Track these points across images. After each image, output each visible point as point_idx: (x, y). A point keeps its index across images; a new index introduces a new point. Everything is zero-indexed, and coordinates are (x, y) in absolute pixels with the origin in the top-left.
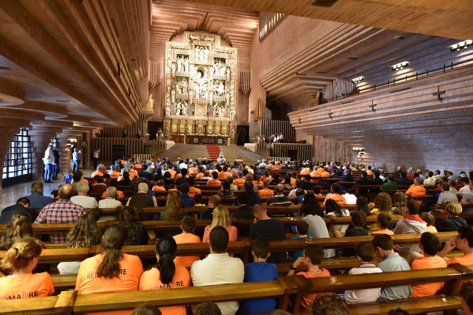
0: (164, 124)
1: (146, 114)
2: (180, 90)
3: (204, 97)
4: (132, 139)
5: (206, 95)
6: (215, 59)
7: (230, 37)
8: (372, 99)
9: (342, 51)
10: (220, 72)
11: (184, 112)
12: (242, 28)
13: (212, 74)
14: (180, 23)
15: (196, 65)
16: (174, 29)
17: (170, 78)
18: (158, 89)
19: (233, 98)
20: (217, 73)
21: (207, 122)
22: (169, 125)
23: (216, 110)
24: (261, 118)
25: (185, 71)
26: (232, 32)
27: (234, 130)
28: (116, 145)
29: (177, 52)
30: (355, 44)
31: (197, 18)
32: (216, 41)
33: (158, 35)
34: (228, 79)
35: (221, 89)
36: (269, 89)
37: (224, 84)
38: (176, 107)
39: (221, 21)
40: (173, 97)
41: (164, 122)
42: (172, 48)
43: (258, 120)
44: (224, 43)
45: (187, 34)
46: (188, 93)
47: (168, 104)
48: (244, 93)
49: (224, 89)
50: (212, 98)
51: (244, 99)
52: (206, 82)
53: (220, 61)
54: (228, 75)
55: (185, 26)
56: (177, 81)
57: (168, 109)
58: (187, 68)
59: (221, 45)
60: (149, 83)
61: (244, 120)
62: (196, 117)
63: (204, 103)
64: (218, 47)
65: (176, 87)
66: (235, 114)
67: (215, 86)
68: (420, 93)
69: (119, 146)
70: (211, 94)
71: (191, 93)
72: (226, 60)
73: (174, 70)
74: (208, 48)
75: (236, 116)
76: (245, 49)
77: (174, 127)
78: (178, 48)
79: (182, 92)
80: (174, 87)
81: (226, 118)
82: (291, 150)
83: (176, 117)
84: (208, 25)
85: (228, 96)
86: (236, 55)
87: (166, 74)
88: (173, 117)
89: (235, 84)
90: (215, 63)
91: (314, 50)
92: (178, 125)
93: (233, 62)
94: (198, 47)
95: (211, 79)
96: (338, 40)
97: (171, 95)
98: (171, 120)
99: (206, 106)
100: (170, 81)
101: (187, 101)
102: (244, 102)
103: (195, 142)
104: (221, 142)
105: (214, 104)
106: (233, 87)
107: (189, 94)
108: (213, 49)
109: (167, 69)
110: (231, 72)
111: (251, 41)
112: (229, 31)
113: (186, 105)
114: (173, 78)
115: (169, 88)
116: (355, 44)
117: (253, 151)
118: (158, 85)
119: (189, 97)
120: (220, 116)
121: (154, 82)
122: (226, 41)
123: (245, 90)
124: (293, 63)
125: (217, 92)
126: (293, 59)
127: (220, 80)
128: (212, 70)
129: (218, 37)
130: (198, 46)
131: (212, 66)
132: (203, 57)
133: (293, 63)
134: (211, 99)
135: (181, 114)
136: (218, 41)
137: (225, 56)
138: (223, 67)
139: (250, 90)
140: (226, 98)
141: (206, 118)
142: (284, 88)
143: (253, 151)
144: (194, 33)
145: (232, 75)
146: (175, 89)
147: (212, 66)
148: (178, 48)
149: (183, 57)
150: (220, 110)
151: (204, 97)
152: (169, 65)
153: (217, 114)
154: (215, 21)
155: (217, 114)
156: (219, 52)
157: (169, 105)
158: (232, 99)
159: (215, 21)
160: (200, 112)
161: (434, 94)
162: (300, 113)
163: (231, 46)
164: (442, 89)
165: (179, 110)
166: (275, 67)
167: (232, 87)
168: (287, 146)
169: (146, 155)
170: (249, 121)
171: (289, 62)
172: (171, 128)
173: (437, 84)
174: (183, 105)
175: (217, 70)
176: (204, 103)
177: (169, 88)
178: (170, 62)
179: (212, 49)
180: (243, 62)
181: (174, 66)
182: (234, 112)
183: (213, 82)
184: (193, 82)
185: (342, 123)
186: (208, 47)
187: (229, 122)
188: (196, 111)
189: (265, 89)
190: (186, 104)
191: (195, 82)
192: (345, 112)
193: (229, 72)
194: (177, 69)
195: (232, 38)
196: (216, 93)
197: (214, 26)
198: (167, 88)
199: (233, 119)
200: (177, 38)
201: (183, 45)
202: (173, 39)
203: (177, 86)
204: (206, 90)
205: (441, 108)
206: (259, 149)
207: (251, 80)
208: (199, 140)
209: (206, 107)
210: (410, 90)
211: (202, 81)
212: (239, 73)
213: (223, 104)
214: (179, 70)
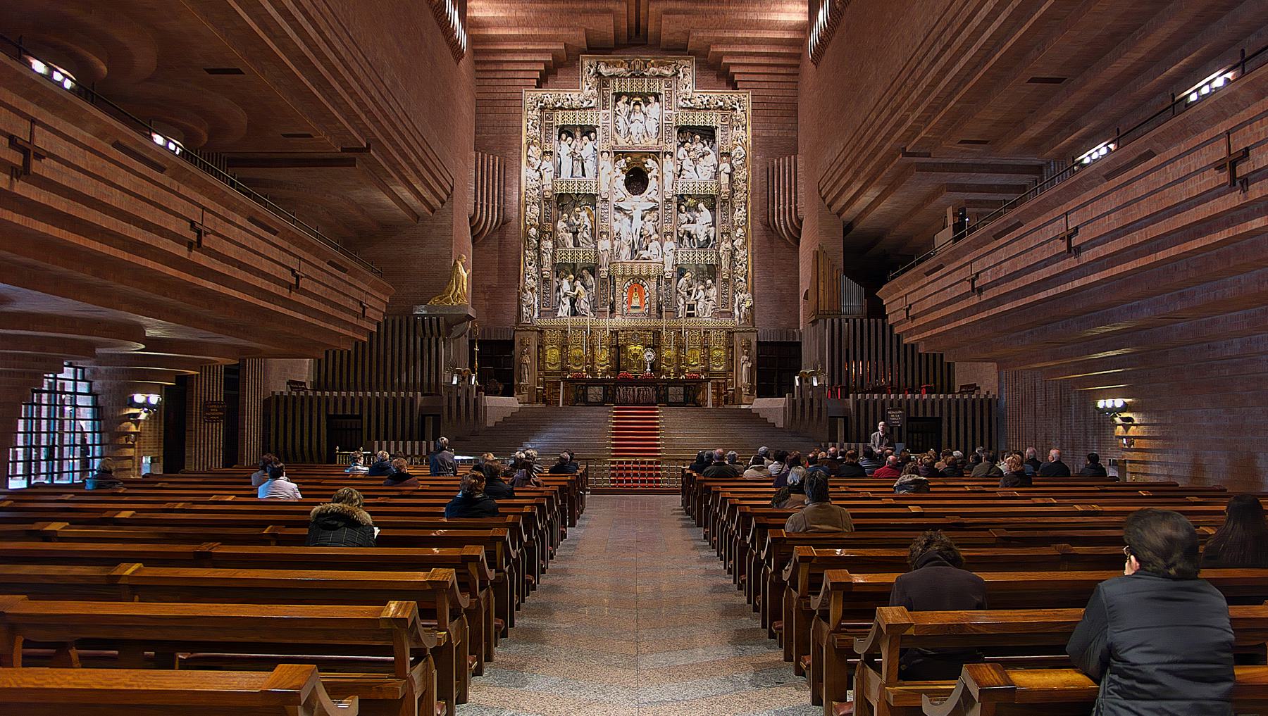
0: (517, 347)
3: (645, 254)
4: (411, 394)
5: (654, 246)
6: (681, 130)
7: (725, 61)
8: (1064, 208)
9: (997, 56)
10: (698, 170)
11: (583, 305)
12: (760, 26)
13: (669, 178)
14: (561, 31)
15: (618, 155)
16: (547, 51)
19: (743, 252)
20: (689, 175)
21: (657, 333)
22: (533, 348)
23: (689, 293)
25: (584, 175)
26: (729, 42)
27: (745, 357)
28: (336, 416)
29: (560, 119)
30: (1027, 26)
31: (609, 11)
32: (681, 75)
33: (499, 75)
34: (725, 189)
35: (702, 224)
36: (848, 215)
37: (712, 209)
38: (558, 290)
39: (685, 12)
40: (547, 258)
41: (517, 341)
42: (542, 109)
44: (711, 78)
45: (586, 63)
47: (531, 283)
48: (776, 239)
49: (714, 225)
50: (672, 256)
52: (653, 205)
54: (724, 179)
55: (577, 37)
56: (561, 208)
57: (532, 299)
58: (589, 166)
59: (699, 85)
62: (618, 321)
64: (687, 91)
65: (555, 229)
66: (748, 304)
67: (684, 217)
68: (1180, 168)
69: (344, 416)
70: (670, 244)
71: (604, 244)
72: (718, 134)
73: (548, 177)
74: (657, 100)
76: (779, 93)
77: (553, 354)
78: (560, 108)
79: (576, 244)
81: (717, 313)
82: (916, 419)
83: (554, 322)
84: (652, 28)
86: (749, 112)
87: (523, 190)
88: (546, 322)
90: (683, 144)
91: (925, 64)
92: (564, 346)
93: (740, 138)
94: (625, 99)
95: (668, 196)
96: (977, 21)
97: (539, 254)
98: (541, 332)
100: (536, 209)
103: (591, 398)
104: (681, 399)
105: (681, 272)
107: (596, 247)
108: (674, 100)
109: (527, 173)
110: (733, 169)
111: (797, 66)
112: (720, 41)
113: (589, 284)
114: (548, 201)
115: (533, 231)
116: (1027, 26)
117: (780, 424)
119: (597, 257)
121: (490, 217)
122: (717, 72)
123: (782, 222)
124: (884, 116)
125: (690, 236)
126: (882, 104)
127: (699, 198)
128: (669, 165)
129: (687, 63)
130: (625, 94)
131: (672, 155)
132: (644, 126)
133: (884, 116)
134: (669, 260)
135: (574, 313)
136: (688, 77)
137: (713, 119)
139: (800, 222)
141: (653, 323)
142: (885, 206)
143: (780, 424)
144: (610, 58)
146: (553, 234)
147: (672, 155)
148: (560, 108)
149: (578, 134)
150: (701, 293)
151: (645, 254)
152: (532, 160)
153: (691, 308)
154: (668, 12)
155: (691, 308)
156: (690, 108)
157: (534, 284)
158: (741, 254)
159: (668, 12)
160: (636, 302)
161: (1219, 167)
162: (907, 285)
163: (733, 85)
164: (1238, 145)
165: (567, 302)
166: (846, 140)
167: (739, 215)
168: (904, 403)
169: (409, 443)
171: (874, 115)
172: (541, 359)
173: (1221, 128)
174: (578, 283)
175: (687, 163)
177: (533, 231)
179: (669, 101)
180: (774, 133)
185: (1007, 307)
186: (657, 97)
187: (730, 333)
188: (619, 301)
189: (839, 214)
191: (619, 209)
192: (1006, 269)
193: (728, 170)
194: (558, 173)
195: (732, 61)
197: (670, 28)
200: (561, 77)
201: (574, 96)
202: (546, 81)
203: (561, 225)
205: (1249, 217)
206: (798, 417)
208: (605, 392)
210: (1154, 161)
211: (638, 204)
213: (712, 271)
214: (566, 174)
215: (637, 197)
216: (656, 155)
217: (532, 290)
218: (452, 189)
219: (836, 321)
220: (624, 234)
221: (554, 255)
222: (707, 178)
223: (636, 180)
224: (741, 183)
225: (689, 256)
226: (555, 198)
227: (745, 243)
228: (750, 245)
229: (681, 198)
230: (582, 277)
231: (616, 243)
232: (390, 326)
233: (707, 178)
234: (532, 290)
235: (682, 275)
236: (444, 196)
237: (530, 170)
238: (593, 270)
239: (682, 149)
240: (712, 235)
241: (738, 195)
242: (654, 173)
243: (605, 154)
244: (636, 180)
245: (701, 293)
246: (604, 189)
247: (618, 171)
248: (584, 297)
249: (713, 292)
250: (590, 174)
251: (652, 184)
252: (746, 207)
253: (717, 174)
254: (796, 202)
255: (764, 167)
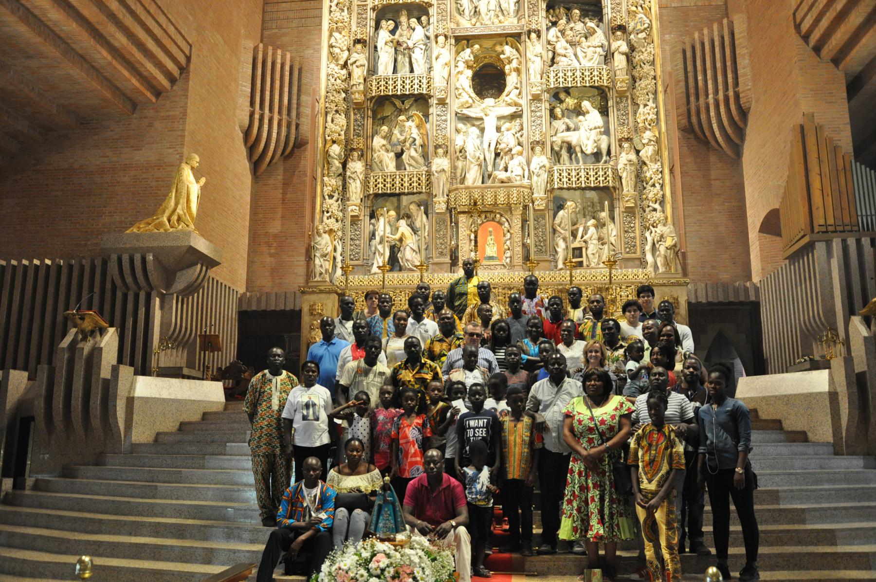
1: (159, 252)
2: (389, 162)
13: (536, 66)
15: (462, 41)
17: (343, 106)
18: (296, 166)
24: (827, 234)
25: (412, 71)
34: (622, 76)
35: (588, 130)
37: (604, 111)
38: (373, 235)
40: (355, 189)
41: (306, 309)
43: (809, 247)
46: (428, 164)
48: (709, 141)
50: (545, 176)
51: (714, 174)
52: (513, 109)
53: (577, 12)
54: (620, 61)
56: (380, 120)
58: (418, 56)
60: (247, 133)
61: (725, 277)
63: (501, 199)
66: (669, 242)
67: (560, 124)
70: (540, 160)
71: (440, 163)
73: (358, 74)
75: (678, 253)
79: (400, 165)
80: (358, 143)
85: (625, 158)
89: (661, 97)
95: (536, 91)
99: (518, 213)
100: (341, 120)
101: (426, 206)
102: (716, 184)
106: (653, 115)
110: (632, 48)
113: (418, 224)
114: (358, 107)
118: (295, 147)
119: (429, 184)
120: (594, 261)
121: (274, 134)
125: (570, 149)
128: (535, 49)
131: (539, 34)
134: (539, 183)
138: (595, 32)
139: (744, 114)
140: (615, 171)
145: (637, 57)
146: (365, 154)
147: (539, 34)
157: (336, 226)
167: (645, 113)
170: (756, 279)
175: (561, 46)
176: (501, 199)
177: (336, 150)
178: (342, 40)
181: (360, 57)
182: (663, 232)
183: (545, 106)
184: (450, 116)
189: (836, 61)
190: (421, 219)
191: (465, 119)
193: (624, 48)
194: (372, 70)
196: (564, 154)
198: (326, 153)
199: (661, 269)
204: (512, 142)
207: (744, 63)
209: (517, 223)
211: (491, 109)
212: (674, 54)
215: (489, 101)
216: (515, 38)
217: (331, 232)
218: (189, 59)
219: (851, 242)
220: (470, 150)
221: (366, 184)
222: (594, 64)
223: (489, 80)
224: (647, 68)
225: (571, 171)
226: (370, 105)
227: (658, 152)
228: (666, 154)
229: (557, 95)
230: (408, 216)
231: (460, 164)
232: (75, 274)
233: (594, 64)
234: (331, 232)
235: (561, 207)
236: (175, 71)
237: (332, 66)
238: (426, 206)
239: (554, 31)
240: (604, 148)
241: (643, 83)
242: (514, 64)
243: (441, 39)
244: (489, 80)
245: (592, 230)
246: (439, 82)
247: (462, 66)
248: (411, 241)
249: (612, 231)
250: (420, 68)
251: (511, 80)
252: (655, 99)
253: (608, 57)
254: (736, 84)
255: (679, 47)
